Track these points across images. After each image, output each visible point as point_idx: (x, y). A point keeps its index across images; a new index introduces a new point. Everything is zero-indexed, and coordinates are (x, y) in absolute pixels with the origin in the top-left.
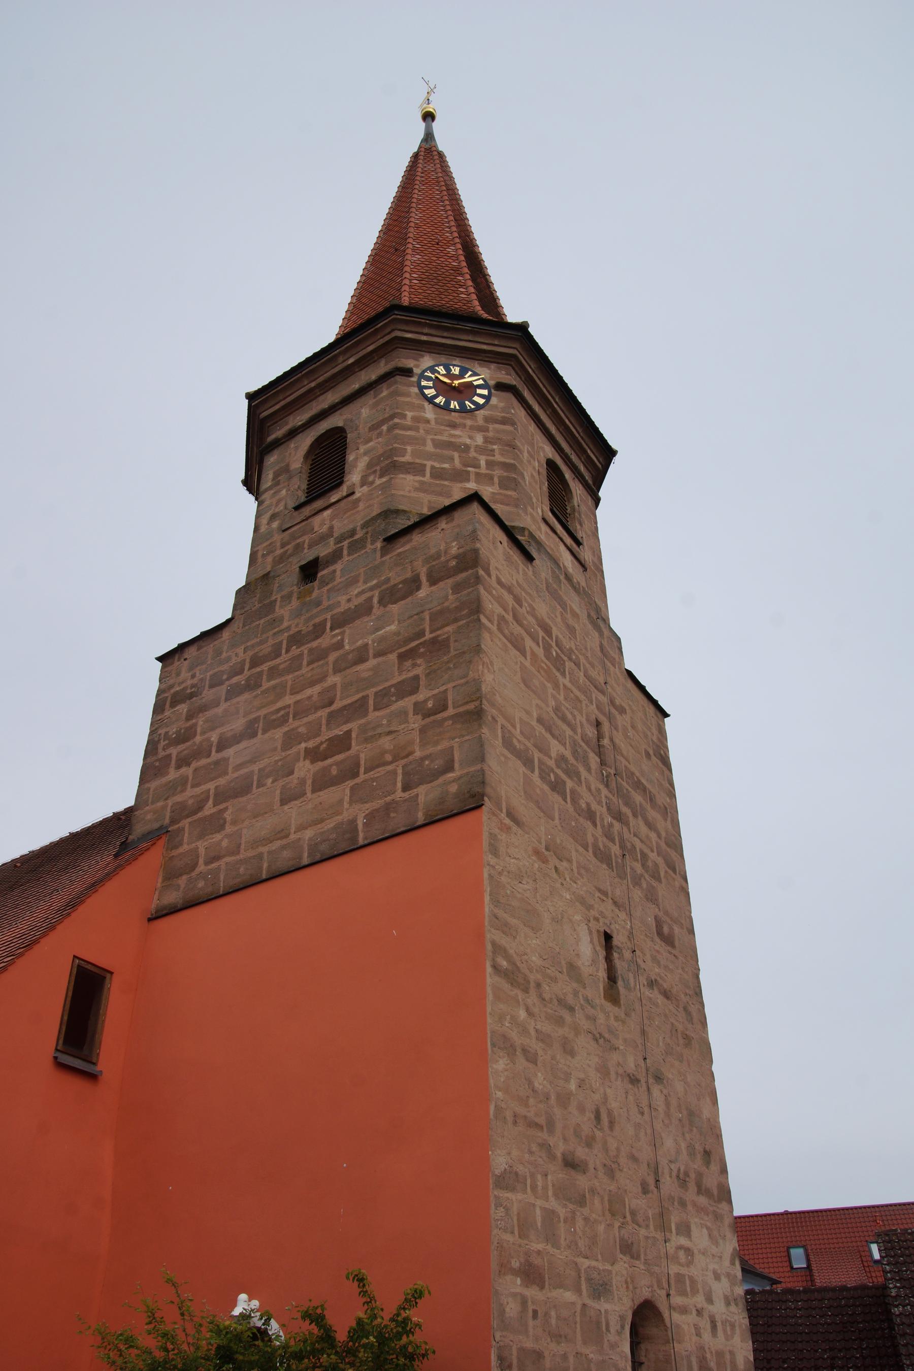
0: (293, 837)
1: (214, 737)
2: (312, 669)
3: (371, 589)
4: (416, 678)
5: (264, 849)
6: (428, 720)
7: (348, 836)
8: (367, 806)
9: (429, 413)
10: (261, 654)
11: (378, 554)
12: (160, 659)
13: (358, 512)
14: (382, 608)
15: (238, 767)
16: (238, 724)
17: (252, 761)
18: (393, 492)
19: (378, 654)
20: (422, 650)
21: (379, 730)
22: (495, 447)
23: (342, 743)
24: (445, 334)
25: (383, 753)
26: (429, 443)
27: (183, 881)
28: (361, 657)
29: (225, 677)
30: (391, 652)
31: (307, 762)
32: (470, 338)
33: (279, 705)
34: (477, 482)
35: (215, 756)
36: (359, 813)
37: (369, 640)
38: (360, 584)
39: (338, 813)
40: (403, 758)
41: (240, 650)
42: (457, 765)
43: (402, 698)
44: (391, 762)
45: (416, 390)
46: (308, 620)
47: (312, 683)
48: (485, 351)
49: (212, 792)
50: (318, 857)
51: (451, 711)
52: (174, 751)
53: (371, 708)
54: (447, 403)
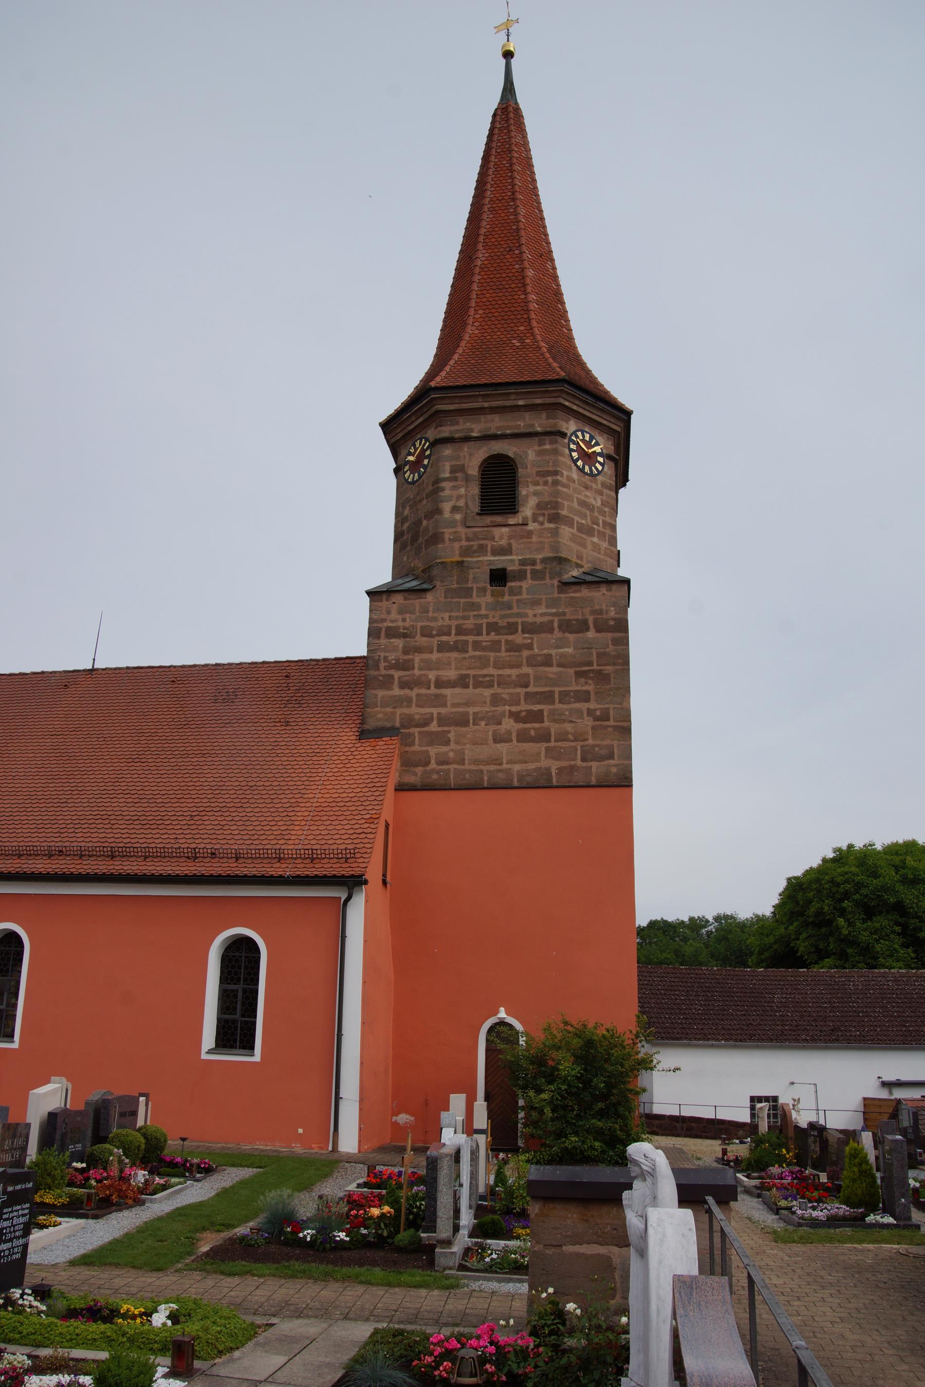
0: (505, 766)
1: (432, 675)
2: (510, 656)
4: (588, 692)
5: (485, 768)
7: (544, 777)
8: (558, 763)
9: (575, 475)
10: (464, 627)
11: (556, 590)
12: (369, 593)
13: (531, 542)
14: (561, 633)
15: (455, 705)
16: (451, 674)
17: (467, 704)
18: (560, 540)
19: (560, 665)
21: (563, 717)
22: (606, 509)
23: (537, 717)
24: (587, 408)
25: (567, 733)
26: (575, 500)
27: (419, 770)
28: (547, 661)
29: (434, 632)
30: (572, 667)
31: (512, 720)
32: (599, 414)
33: (485, 672)
35: (433, 690)
36: (554, 766)
37: (553, 652)
38: (543, 606)
39: (538, 761)
40: (581, 741)
41: (446, 615)
42: (616, 757)
43: (579, 702)
44: (572, 741)
45: (567, 451)
46: (502, 617)
48: (604, 425)
49: (435, 716)
50: (524, 784)
51: (611, 723)
52: (397, 674)
53: (557, 701)
54: (577, 460)
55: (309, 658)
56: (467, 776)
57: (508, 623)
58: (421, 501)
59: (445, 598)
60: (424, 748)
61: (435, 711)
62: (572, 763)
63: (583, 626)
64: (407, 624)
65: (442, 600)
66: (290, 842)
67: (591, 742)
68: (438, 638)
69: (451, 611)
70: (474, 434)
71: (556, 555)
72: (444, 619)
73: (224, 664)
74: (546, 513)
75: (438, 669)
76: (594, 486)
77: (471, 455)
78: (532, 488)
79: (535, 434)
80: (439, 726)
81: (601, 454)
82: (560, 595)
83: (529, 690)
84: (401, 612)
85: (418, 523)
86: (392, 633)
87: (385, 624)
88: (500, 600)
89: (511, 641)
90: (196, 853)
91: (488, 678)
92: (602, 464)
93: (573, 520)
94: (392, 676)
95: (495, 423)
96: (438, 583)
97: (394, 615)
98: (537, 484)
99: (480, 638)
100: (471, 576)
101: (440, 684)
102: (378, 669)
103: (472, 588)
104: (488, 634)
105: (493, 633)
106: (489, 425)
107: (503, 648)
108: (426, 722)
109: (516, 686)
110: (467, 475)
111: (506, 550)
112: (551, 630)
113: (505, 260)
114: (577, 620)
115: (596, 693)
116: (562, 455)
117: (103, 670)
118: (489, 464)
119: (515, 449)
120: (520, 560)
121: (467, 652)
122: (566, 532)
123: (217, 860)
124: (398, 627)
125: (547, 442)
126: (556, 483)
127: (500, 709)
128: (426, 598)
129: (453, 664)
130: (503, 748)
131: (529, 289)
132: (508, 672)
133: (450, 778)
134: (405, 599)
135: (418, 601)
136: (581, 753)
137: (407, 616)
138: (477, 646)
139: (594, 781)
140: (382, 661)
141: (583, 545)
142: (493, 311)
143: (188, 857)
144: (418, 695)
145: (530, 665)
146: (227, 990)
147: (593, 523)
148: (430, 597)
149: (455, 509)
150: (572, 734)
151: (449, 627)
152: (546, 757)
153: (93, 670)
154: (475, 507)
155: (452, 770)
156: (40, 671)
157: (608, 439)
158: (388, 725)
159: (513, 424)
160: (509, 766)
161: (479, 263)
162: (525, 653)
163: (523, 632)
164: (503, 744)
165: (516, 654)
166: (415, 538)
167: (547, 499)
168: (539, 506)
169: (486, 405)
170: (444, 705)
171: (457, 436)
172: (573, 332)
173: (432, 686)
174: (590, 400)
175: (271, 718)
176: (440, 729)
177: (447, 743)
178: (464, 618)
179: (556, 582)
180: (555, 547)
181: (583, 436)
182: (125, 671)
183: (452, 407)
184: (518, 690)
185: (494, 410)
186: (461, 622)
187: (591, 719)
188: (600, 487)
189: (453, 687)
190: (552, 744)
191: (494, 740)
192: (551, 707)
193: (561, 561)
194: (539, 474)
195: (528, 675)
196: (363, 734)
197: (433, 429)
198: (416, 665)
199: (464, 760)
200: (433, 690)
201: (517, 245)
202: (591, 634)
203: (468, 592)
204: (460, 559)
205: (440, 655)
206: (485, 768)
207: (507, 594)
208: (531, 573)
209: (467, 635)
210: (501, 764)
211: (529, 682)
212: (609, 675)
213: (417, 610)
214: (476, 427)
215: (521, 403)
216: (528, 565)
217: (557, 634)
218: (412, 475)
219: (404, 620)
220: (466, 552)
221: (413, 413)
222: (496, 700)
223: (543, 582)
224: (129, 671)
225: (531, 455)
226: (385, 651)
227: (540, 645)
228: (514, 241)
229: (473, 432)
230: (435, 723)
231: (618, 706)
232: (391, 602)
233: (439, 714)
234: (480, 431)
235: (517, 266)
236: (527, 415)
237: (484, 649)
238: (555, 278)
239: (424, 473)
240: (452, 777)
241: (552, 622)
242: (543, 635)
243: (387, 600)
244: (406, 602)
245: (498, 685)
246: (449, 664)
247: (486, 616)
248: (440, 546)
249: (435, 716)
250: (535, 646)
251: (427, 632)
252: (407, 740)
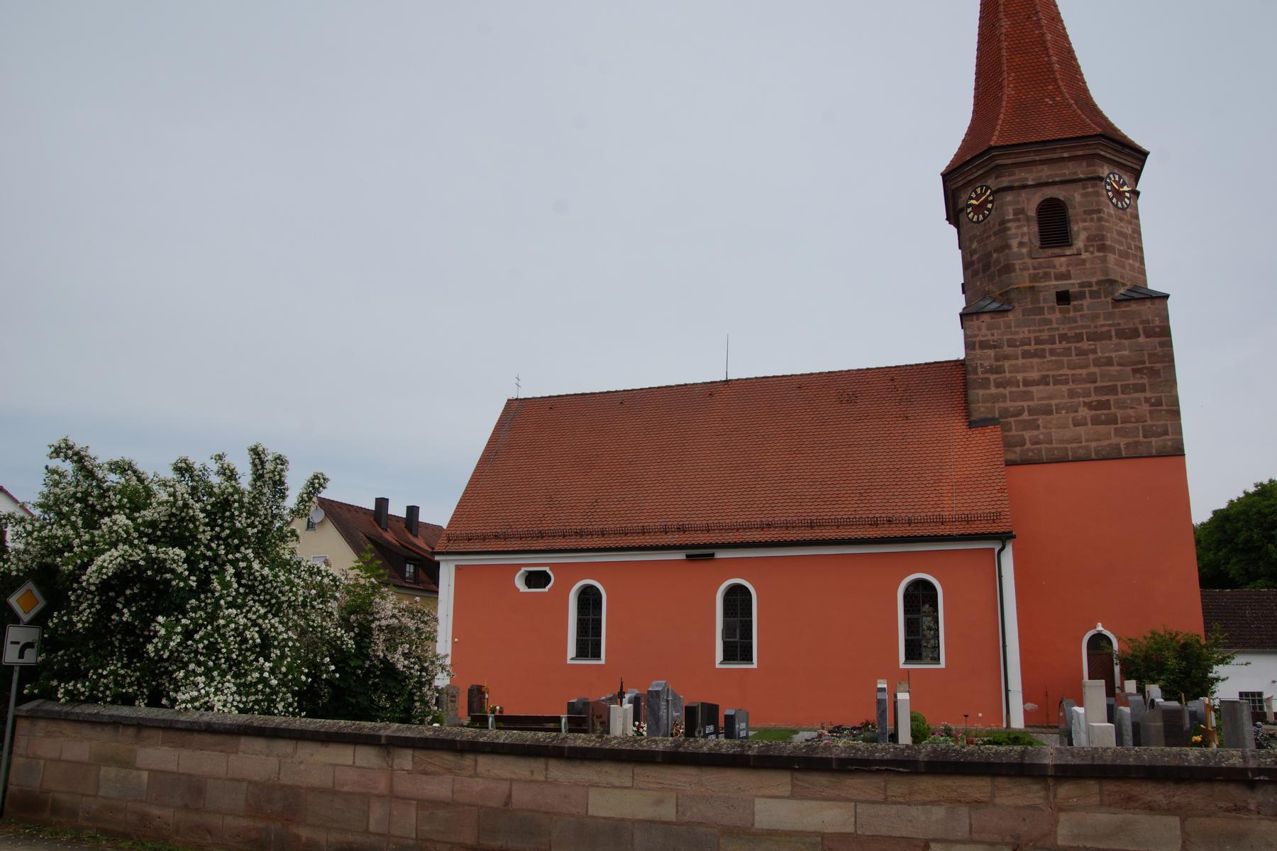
0: (1084, 444)
1: (1020, 377)
3: (1109, 325)
4: (1143, 385)
5: (1069, 446)
6: (1153, 408)
9: (1112, 212)
10: (1041, 338)
11: (1110, 306)
13: (1086, 268)
15: (1040, 399)
16: (1035, 375)
17: (1050, 398)
20: (1145, 371)
21: (1126, 405)
23: (1105, 405)
24: (1116, 154)
25: (1130, 417)
27: (1018, 449)
28: (1109, 362)
29: (1018, 343)
30: (1129, 366)
31: (1086, 409)
32: (1125, 157)
33: (1061, 372)
34: (1133, 260)
35: (1022, 388)
36: (1122, 442)
37: (1113, 355)
41: (1026, 330)
42: (1170, 433)
45: (1105, 192)
47: (1081, 367)
49: (1026, 408)
50: (1101, 457)
51: (1164, 407)
52: (992, 377)
53: (1120, 392)
55: (904, 364)
56: (1056, 452)
57: (1075, 333)
58: (988, 237)
59: (1023, 315)
60: (1020, 433)
61: (1025, 404)
62: (1136, 439)
63: (1134, 334)
64: (995, 338)
65: (1021, 317)
66: (946, 509)
67: (1149, 422)
68: (1021, 348)
69: (1029, 326)
70: (1030, 183)
71: (1107, 278)
72: (1024, 333)
73: (835, 372)
74: (1094, 243)
75: (1024, 372)
76: (1125, 217)
77: (1029, 199)
78: (1081, 225)
79: (1080, 180)
80: (1029, 415)
81: (1128, 192)
82: (1115, 310)
83: (1097, 385)
84: (989, 329)
85: (989, 255)
86: (984, 345)
87: (978, 339)
88: (1067, 315)
89: (1080, 347)
90: (877, 521)
91: (1064, 377)
92: (1129, 199)
93: (1115, 247)
94: (988, 379)
95: (1045, 173)
96: (1016, 305)
97: (984, 331)
98: (1085, 221)
99: (1054, 346)
100: (1041, 298)
101: (1027, 383)
102: (976, 373)
103: (1044, 307)
104: (1060, 343)
105: (1064, 342)
106: (1041, 174)
107: (1073, 353)
108: (1019, 413)
109: (1087, 382)
110: (1027, 216)
111: (1067, 276)
112: (1110, 338)
113: (1025, 27)
114: (1130, 329)
115: (1150, 385)
116: (1102, 195)
117: (736, 380)
118: (1043, 206)
119: (1064, 193)
120: (1079, 283)
121: (1045, 357)
122: (1112, 257)
123: (894, 525)
124: (989, 341)
125: (1090, 186)
126: (1100, 219)
127: (1076, 400)
128: (1008, 317)
129: (1035, 367)
130: (1081, 430)
131: (1051, 52)
132: (1079, 371)
133: (1042, 454)
134: (992, 318)
135: (1002, 319)
136: (1143, 432)
137: (995, 332)
138: (1052, 352)
139: (1154, 452)
140: (979, 367)
141: (1123, 267)
142: (1024, 73)
143: (871, 524)
144: (1011, 392)
145: (1095, 365)
146: (910, 619)
147: (1129, 248)
148: (1011, 316)
149: (1021, 244)
150: (1134, 417)
151: (1029, 338)
152: (1115, 436)
153: (727, 381)
154: (1036, 242)
155: (1043, 449)
156: (683, 383)
157: (1131, 176)
158: (990, 416)
159: (1059, 172)
160: (1088, 444)
161: (1004, 31)
162: (1091, 357)
163: (1088, 340)
164: (1081, 427)
165: (1084, 357)
166: (986, 268)
167: (1094, 232)
168: (1088, 239)
169: (1037, 158)
170: (1032, 399)
171: (1016, 184)
172: (1087, 84)
173: (1021, 384)
174: (1119, 148)
175: (892, 415)
176: (1031, 417)
177: (1038, 428)
178: (1040, 331)
179: (1109, 299)
180: (1105, 271)
181: (1114, 178)
182: (755, 381)
183: (1009, 161)
184: (1089, 385)
185: (1043, 162)
186: (1038, 334)
187: (1148, 405)
188: (1129, 218)
189: (1038, 385)
190: (1120, 425)
191: (1073, 424)
192: (1116, 397)
193: (1112, 282)
194: (1085, 212)
195: (1095, 373)
196: (971, 425)
197: (993, 179)
198: (1006, 369)
199: (1052, 440)
200: (1022, 388)
201: (1034, 12)
202: (1142, 339)
203: (1040, 311)
204: (1031, 285)
205: (1024, 361)
206: (1069, 446)
207: (1072, 311)
208: (1089, 293)
209: (1044, 344)
210: (1081, 442)
211: (1097, 378)
212: (1159, 370)
213: (1002, 327)
214: (1030, 177)
215: (1066, 155)
216: (1085, 287)
217: (1115, 340)
218: (976, 216)
219: (993, 335)
220: (1034, 278)
222: (1072, 394)
223: (1100, 300)
224: (758, 380)
225: (1078, 197)
226: (980, 359)
227: (1104, 349)
228: (1031, 9)
229: (1027, 180)
230: (1026, 413)
231: (1169, 394)
232: (980, 321)
233: (1028, 406)
234: (1033, 180)
235: (1037, 32)
236: (1070, 164)
237: (1059, 355)
238: (1066, 37)
239: (988, 215)
240: (1044, 453)
241: (1110, 331)
242: (1104, 342)
243: (977, 319)
244: (993, 320)
245: (1073, 382)
246: (1032, 367)
247: (1057, 329)
248: (1013, 275)
249: (1026, 408)
250: (1099, 351)
251: (1011, 344)
252: (1006, 428)
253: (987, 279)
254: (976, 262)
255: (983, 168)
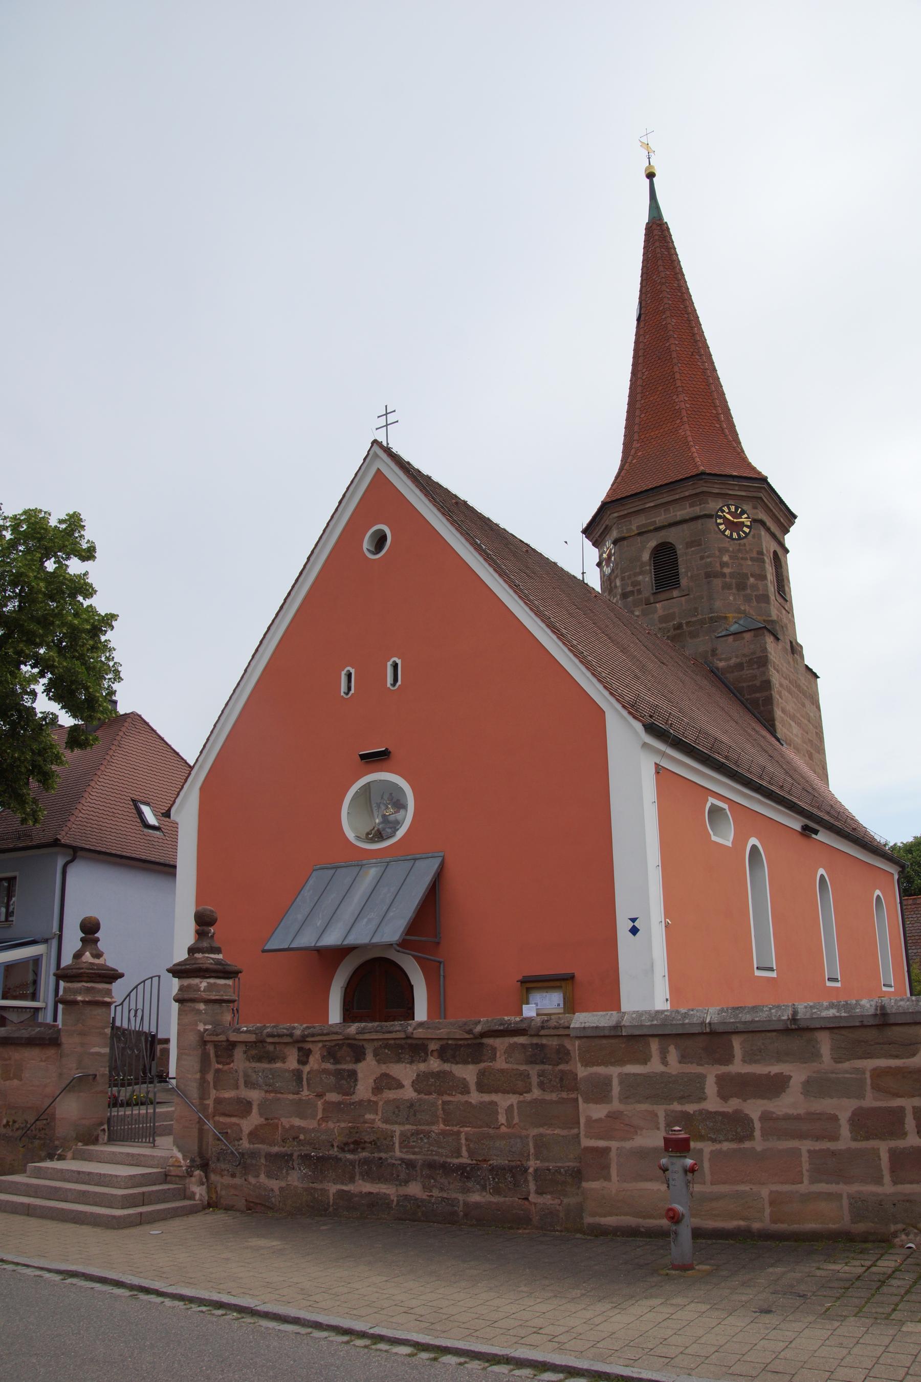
58: (747, 559)
132: (803, 720)
215: (782, 520)
221: (740, 485)
239: (744, 538)
253: (742, 598)
254: (728, 576)
255: (745, 491)
